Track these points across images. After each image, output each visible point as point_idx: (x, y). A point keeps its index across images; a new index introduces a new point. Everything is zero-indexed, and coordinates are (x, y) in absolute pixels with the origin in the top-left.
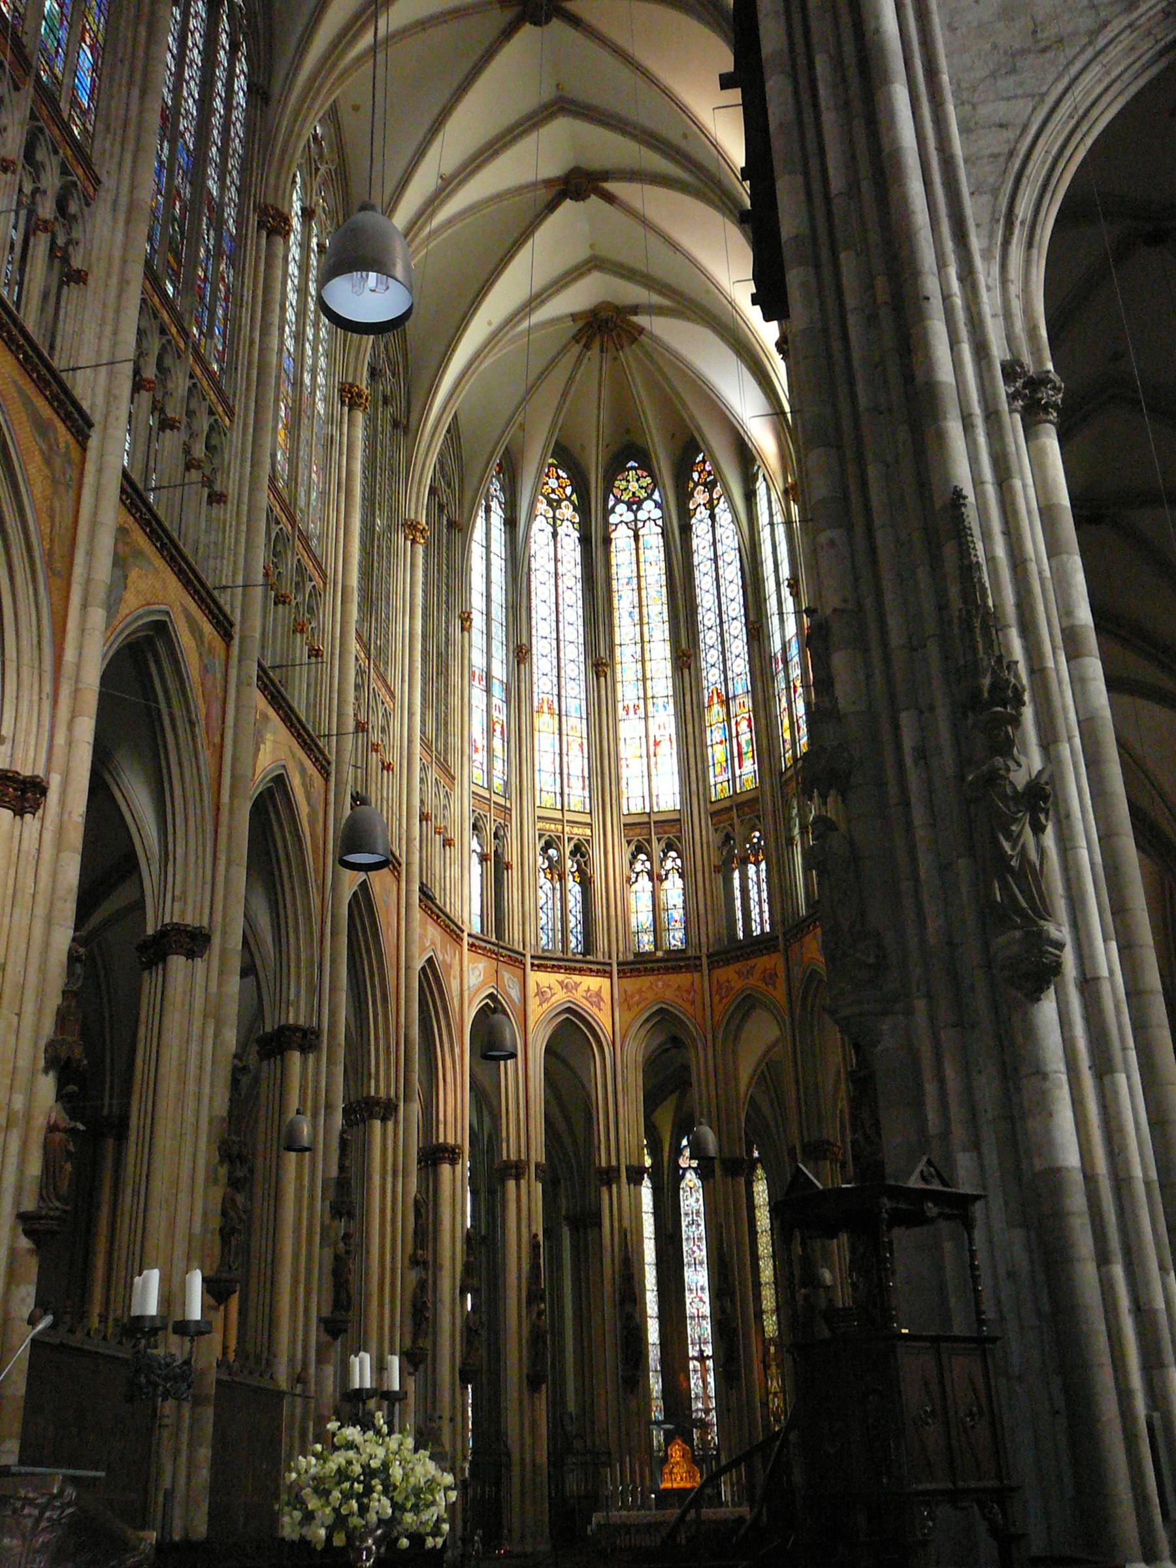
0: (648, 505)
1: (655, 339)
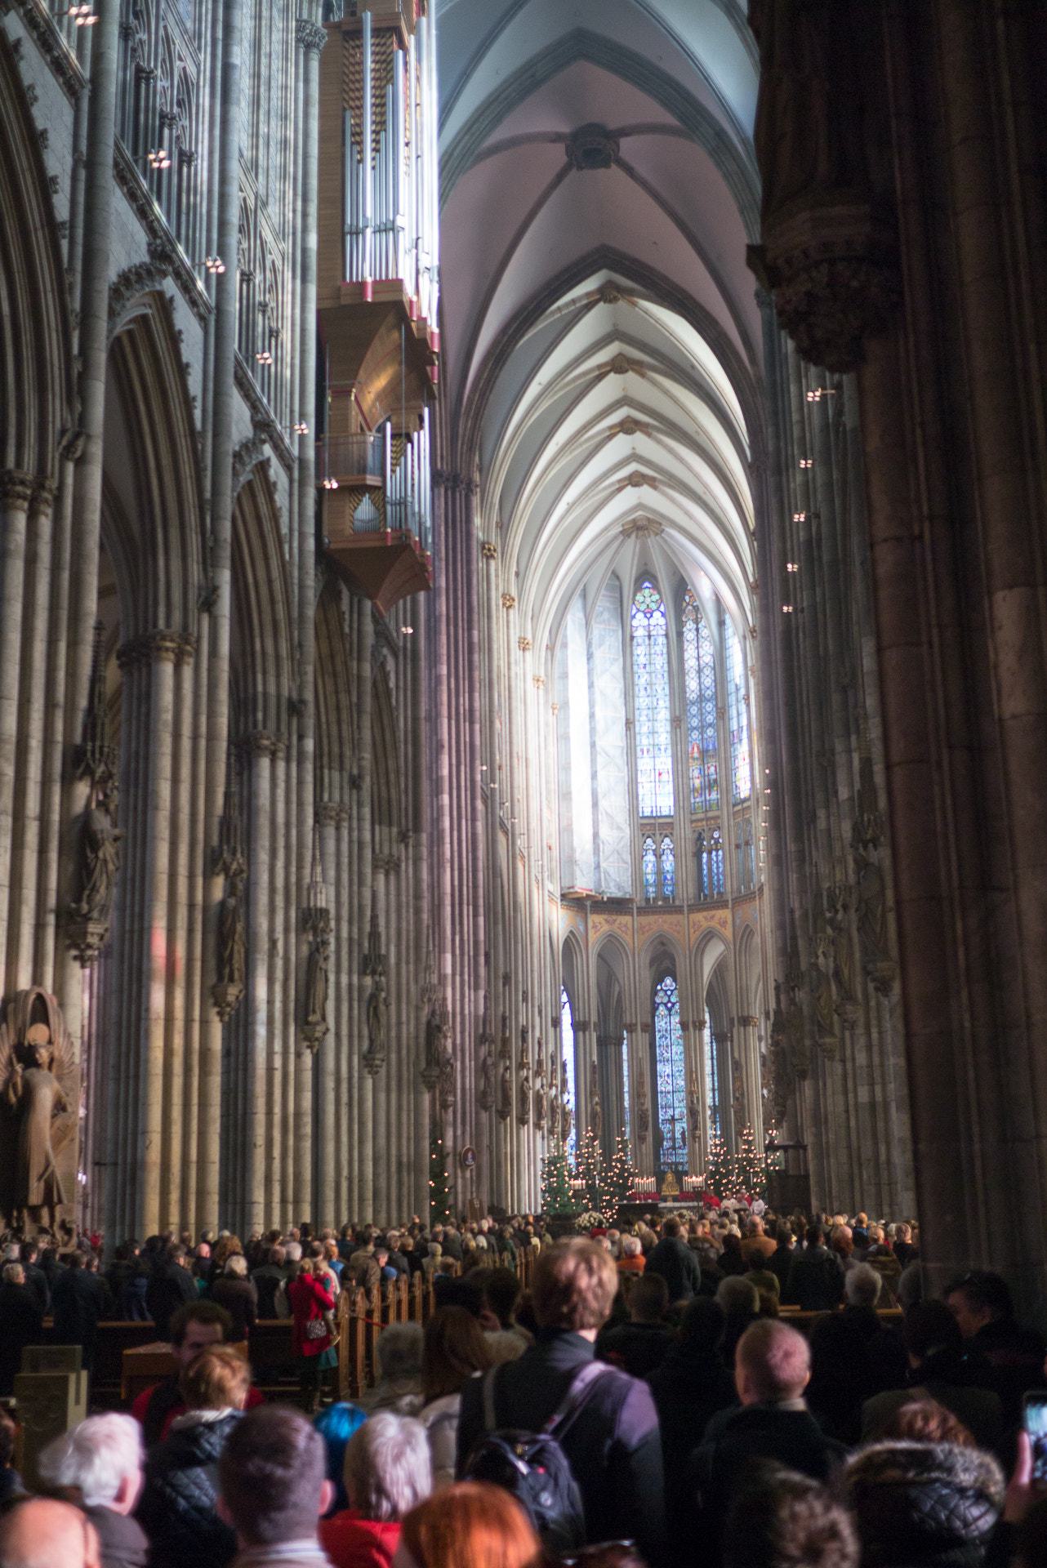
0: (657, 615)
1: (672, 537)
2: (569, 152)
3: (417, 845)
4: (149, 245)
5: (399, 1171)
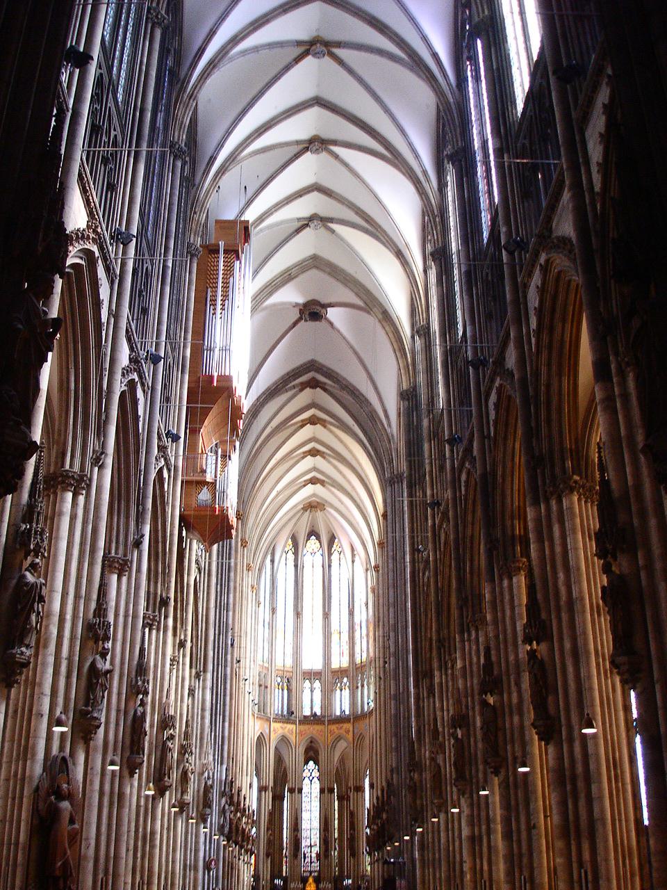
1: (330, 513)
2: (301, 312)
3: (204, 680)
4: (130, 355)
5: (185, 869)
